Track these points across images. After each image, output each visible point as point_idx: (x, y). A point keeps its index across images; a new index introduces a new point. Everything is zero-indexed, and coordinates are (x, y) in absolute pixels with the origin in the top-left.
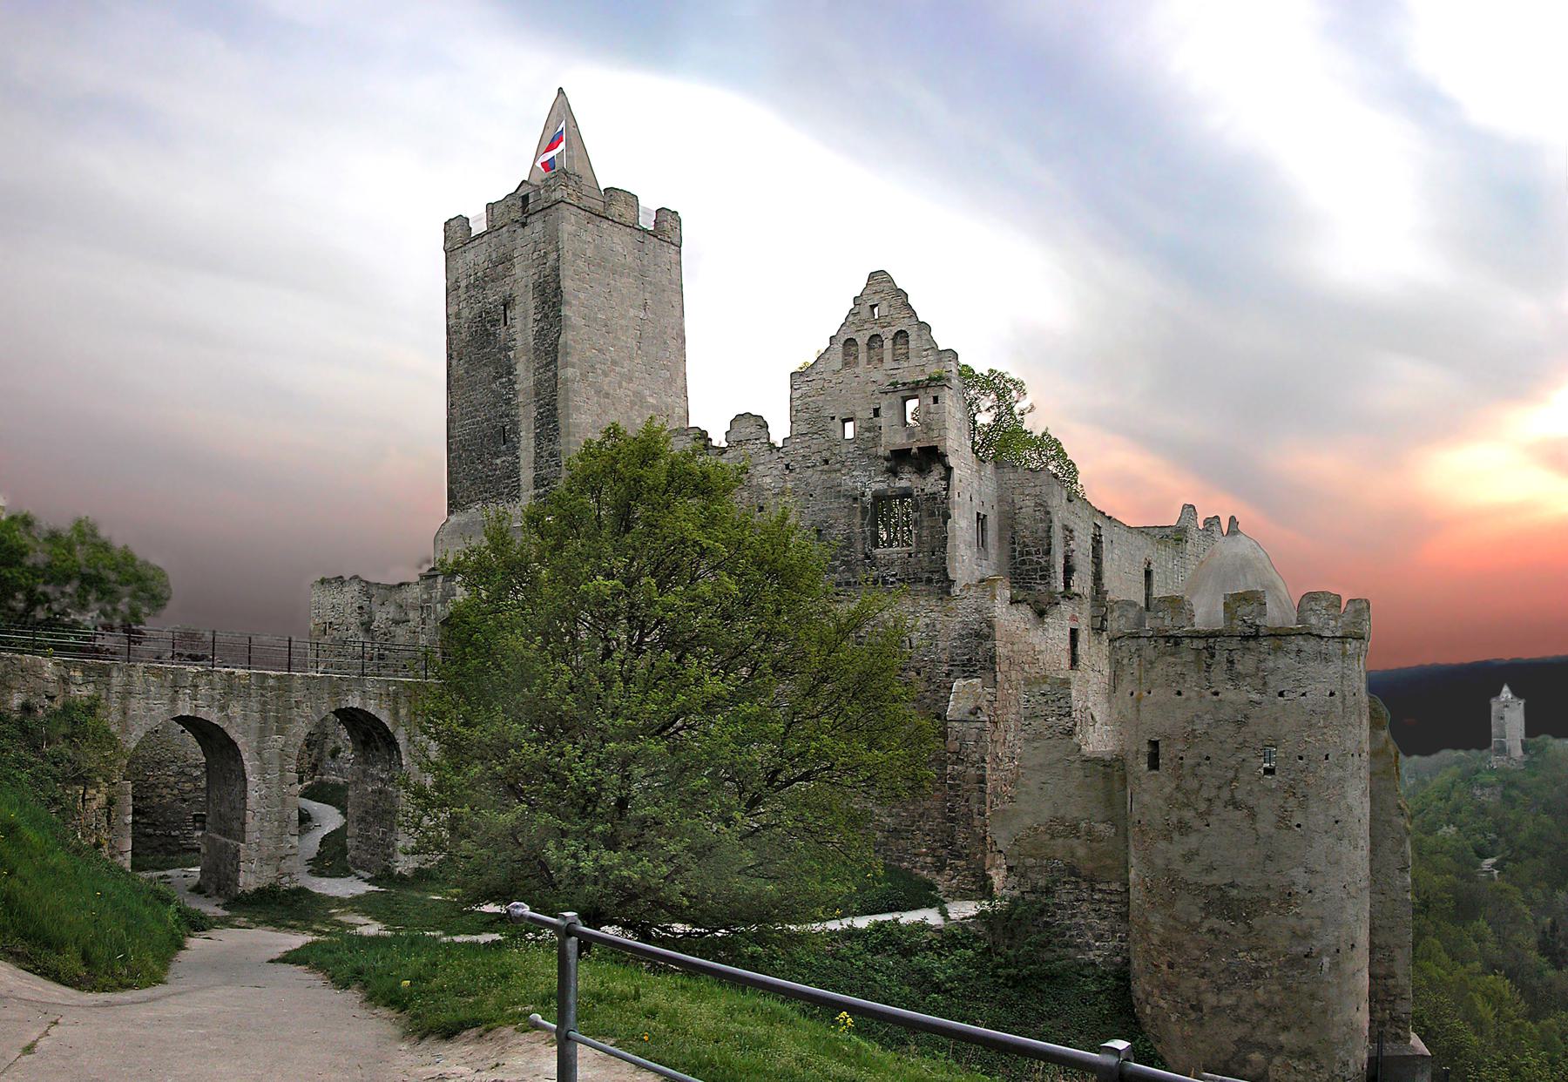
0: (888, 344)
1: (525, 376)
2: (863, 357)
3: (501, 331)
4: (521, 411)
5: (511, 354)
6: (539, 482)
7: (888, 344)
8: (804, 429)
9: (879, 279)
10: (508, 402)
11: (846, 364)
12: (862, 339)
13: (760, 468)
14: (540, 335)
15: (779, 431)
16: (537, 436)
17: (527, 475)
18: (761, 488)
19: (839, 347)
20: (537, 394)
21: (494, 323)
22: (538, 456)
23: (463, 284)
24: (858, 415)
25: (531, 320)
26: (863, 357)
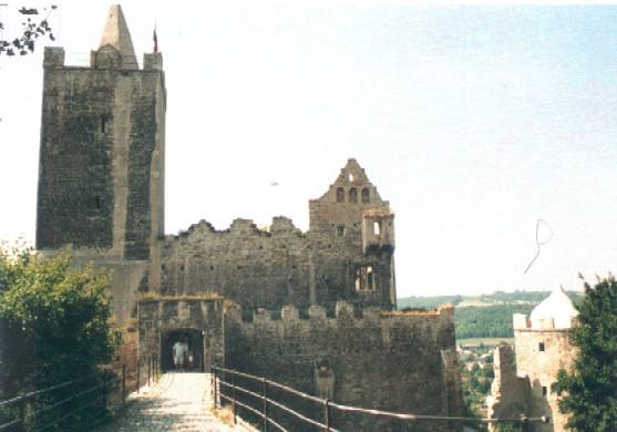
0: (359, 194)
1: (120, 169)
2: (347, 198)
3: (99, 135)
4: (115, 189)
5: (108, 152)
6: (128, 237)
7: (359, 194)
8: (317, 228)
9: (352, 165)
10: (103, 181)
11: (338, 200)
12: (347, 190)
13: (293, 247)
14: (134, 147)
15: (303, 223)
16: (128, 209)
17: (119, 230)
18: (294, 257)
19: (335, 191)
20: (131, 181)
21: (91, 127)
22: (130, 224)
23: (62, 94)
24: (347, 224)
25: (127, 137)
26: (347, 198)
